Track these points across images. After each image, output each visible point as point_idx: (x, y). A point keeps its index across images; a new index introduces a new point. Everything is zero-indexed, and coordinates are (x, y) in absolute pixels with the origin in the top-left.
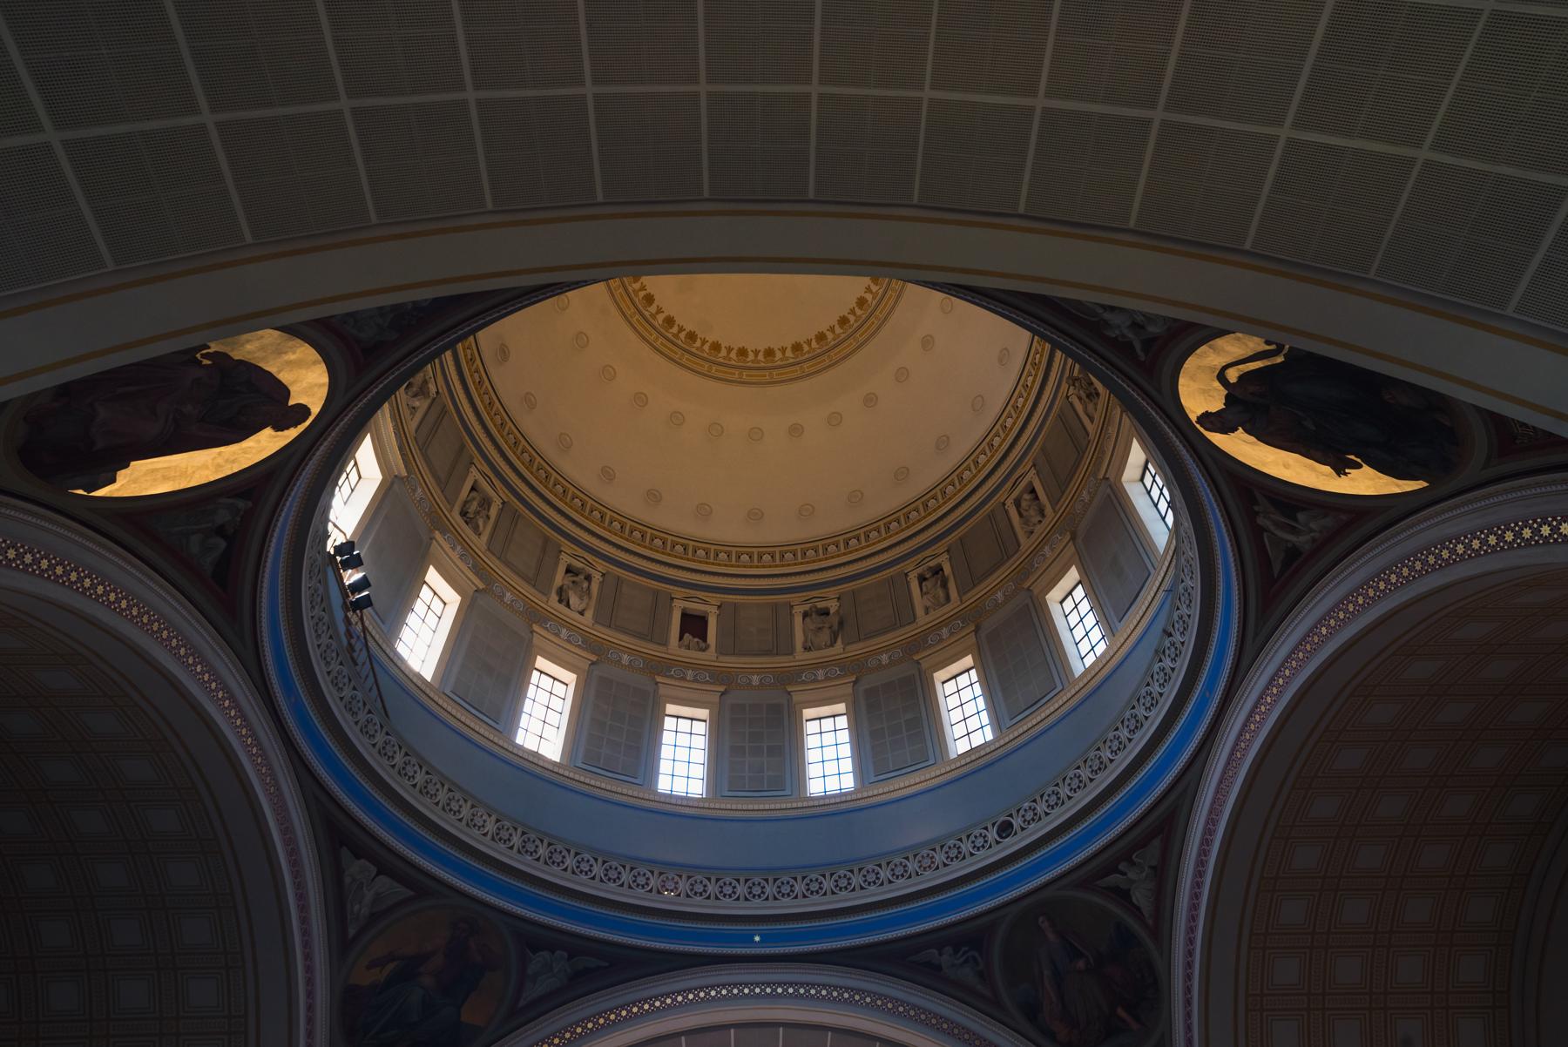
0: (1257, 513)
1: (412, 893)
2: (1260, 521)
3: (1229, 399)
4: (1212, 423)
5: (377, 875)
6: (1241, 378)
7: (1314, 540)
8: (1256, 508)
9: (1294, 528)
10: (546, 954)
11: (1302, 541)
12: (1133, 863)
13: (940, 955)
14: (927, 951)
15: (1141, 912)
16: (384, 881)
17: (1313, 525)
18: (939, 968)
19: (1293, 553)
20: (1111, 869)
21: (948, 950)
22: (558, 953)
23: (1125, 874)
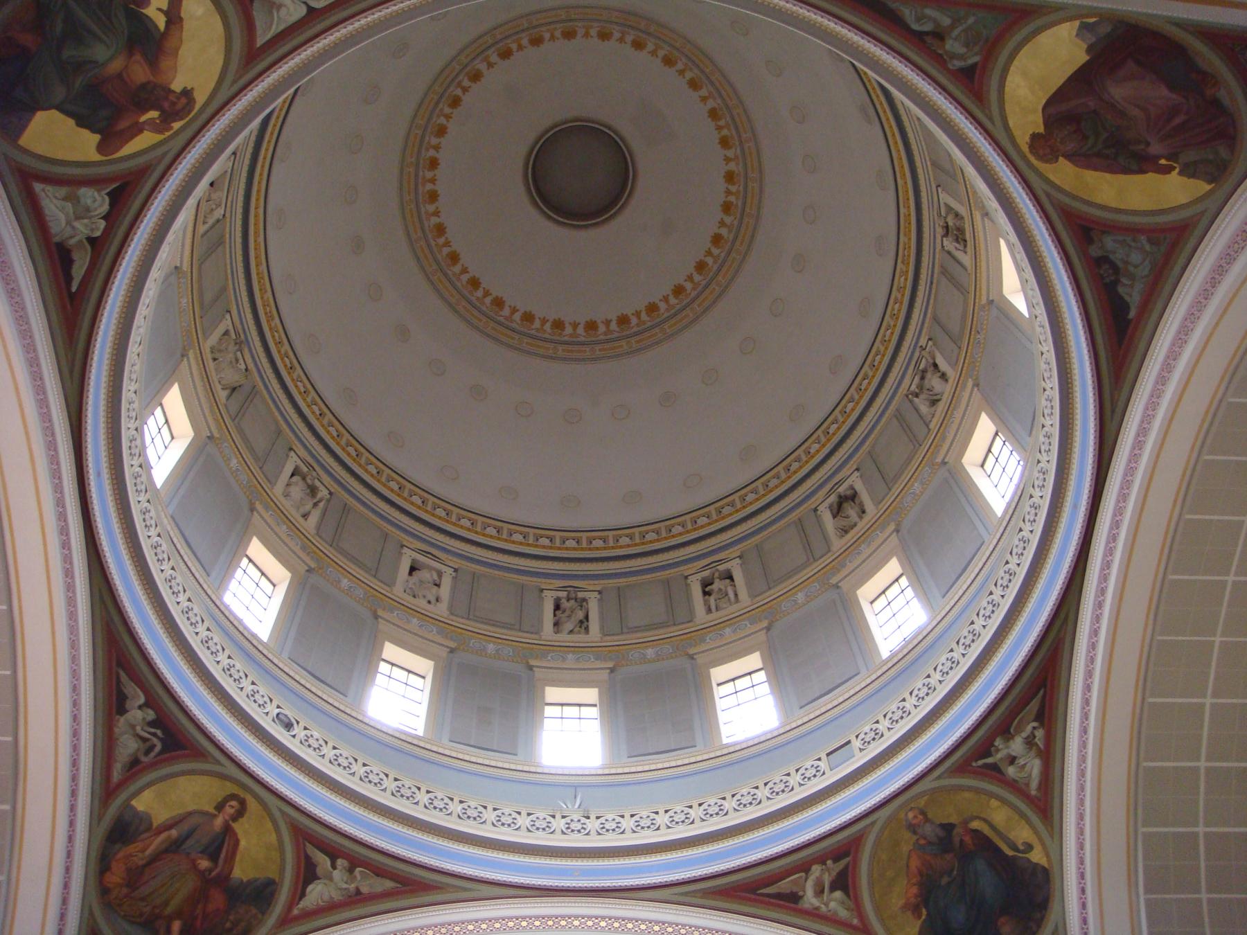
0: (824, 863)
1: (260, 42)
2: (816, 870)
3: (948, 828)
4: (915, 817)
5: (311, 10)
6: (976, 831)
7: (817, 908)
8: (829, 862)
9: (822, 891)
10: (105, 208)
11: (810, 899)
12: (351, 870)
13: (140, 707)
14: (138, 690)
15: (300, 899)
16: (302, 11)
17: (833, 905)
18: (122, 710)
19: (792, 899)
20: (333, 854)
21: (151, 715)
22: (102, 224)
23: (334, 867)
